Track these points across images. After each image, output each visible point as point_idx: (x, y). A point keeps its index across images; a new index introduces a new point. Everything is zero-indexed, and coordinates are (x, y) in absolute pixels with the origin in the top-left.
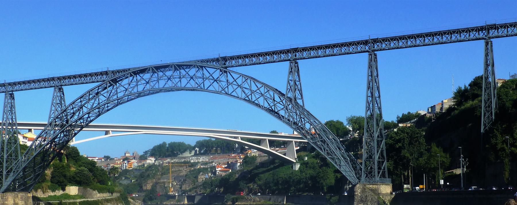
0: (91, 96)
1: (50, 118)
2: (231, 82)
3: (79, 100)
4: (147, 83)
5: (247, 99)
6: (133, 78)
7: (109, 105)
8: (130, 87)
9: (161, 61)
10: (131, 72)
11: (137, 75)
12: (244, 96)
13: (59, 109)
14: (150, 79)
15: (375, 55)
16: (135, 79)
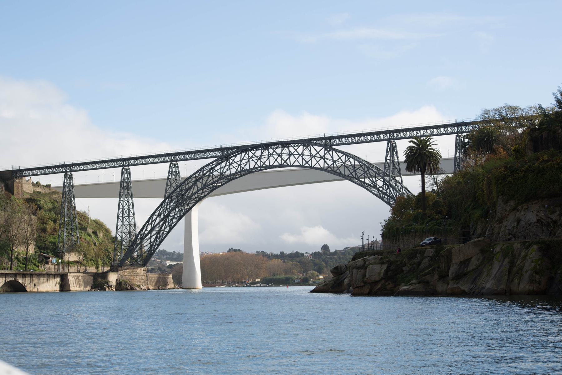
0: (205, 172)
1: (166, 193)
4: (259, 159)
6: (245, 155)
7: (222, 181)
10: (244, 150)
11: (249, 152)
14: (261, 156)
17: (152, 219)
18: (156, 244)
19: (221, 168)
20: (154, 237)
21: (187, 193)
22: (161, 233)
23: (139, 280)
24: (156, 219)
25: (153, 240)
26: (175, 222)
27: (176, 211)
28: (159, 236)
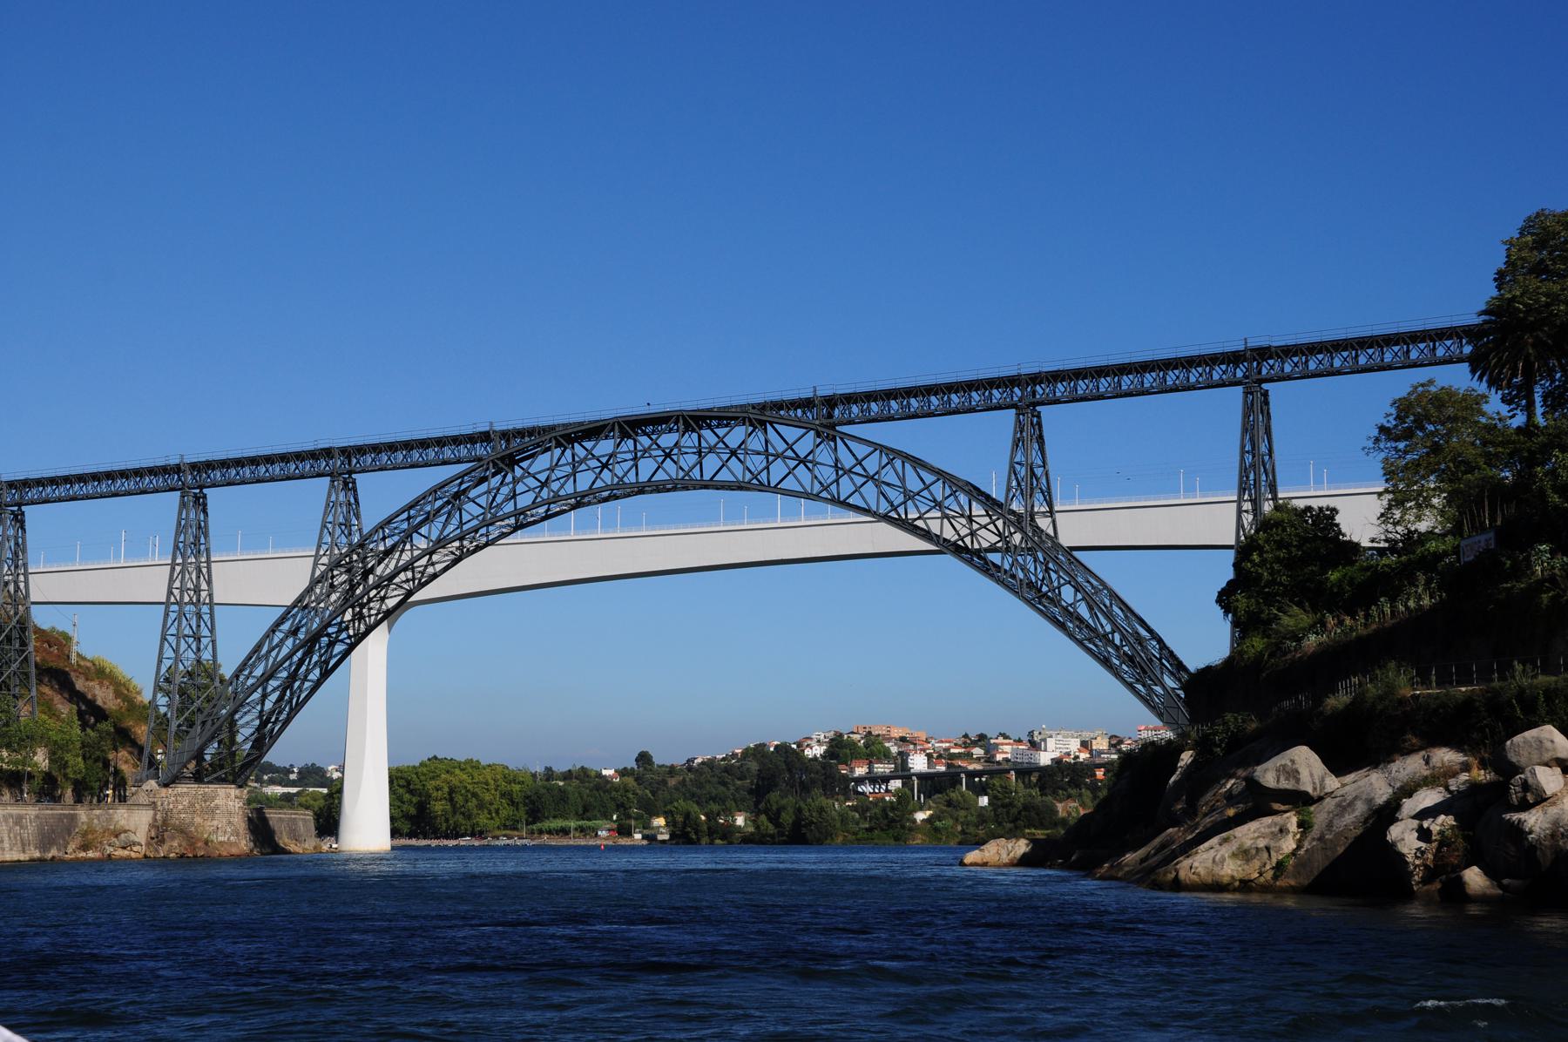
2: (847, 467)
3: (405, 515)
4: (605, 466)
5: (893, 515)
6: (563, 452)
8: (554, 477)
9: (648, 404)
10: (560, 436)
11: (576, 444)
12: (884, 507)
13: (344, 540)
15: (1266, 394)
16: (568, 453)
17: (270, 643)
18: (277, 719)
19: (489, 492)
20: (274, 697)
21: (382, 566)
22: (297, 684)
23: (220, 826)
24: (282, 641)
25: (268, 705)
26: (339, 653)
27: (345, 619)
28: (288, 693)
